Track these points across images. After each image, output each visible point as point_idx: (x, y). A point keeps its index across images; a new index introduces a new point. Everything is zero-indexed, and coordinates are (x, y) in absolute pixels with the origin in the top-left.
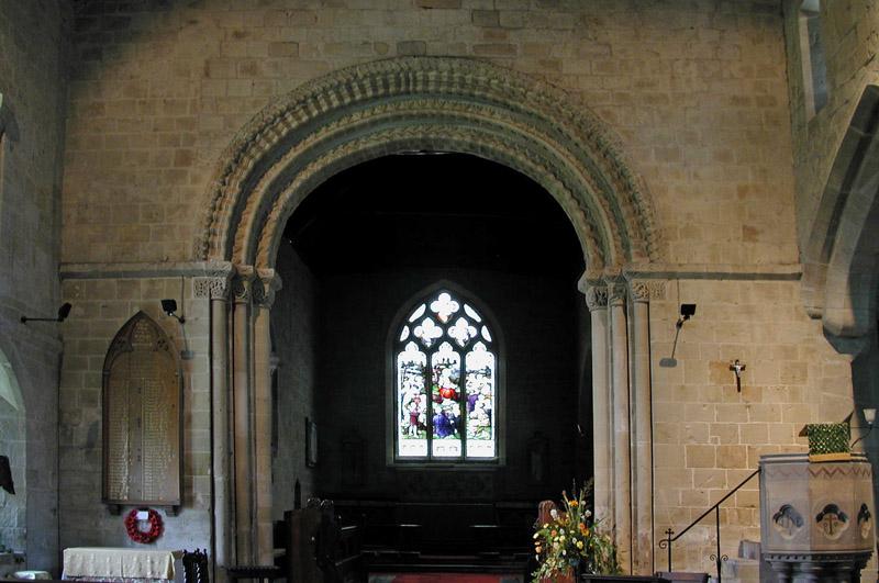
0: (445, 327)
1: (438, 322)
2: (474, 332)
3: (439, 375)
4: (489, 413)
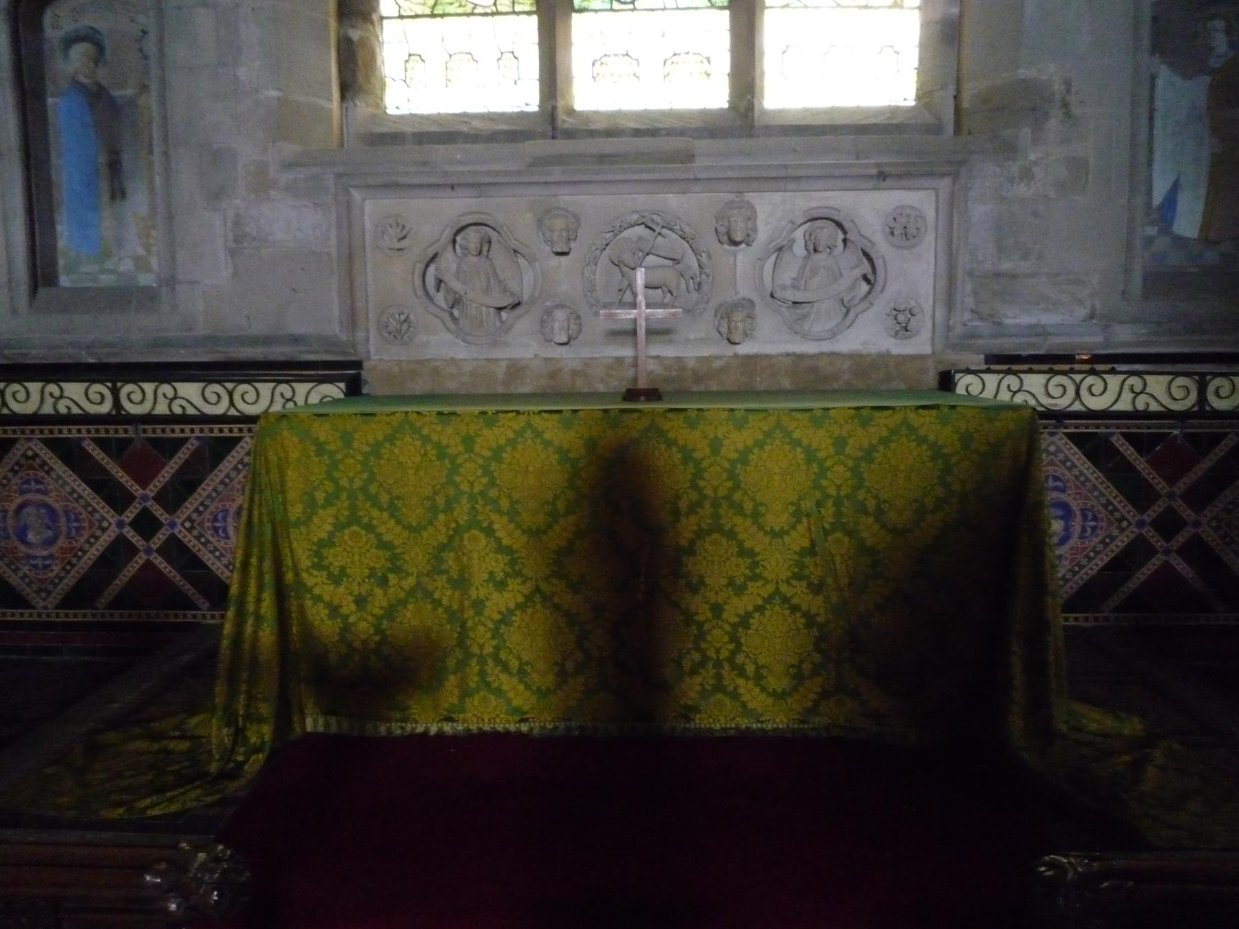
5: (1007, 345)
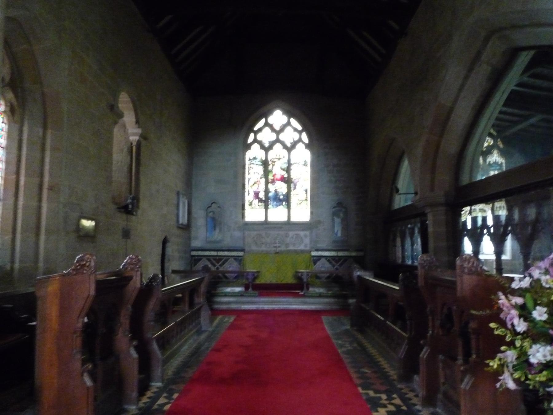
0: (278, 133)
1: (273, 130)
2: (296, 136)
3: (273, 165)
4: (306, 191)
5: (317, 248)
